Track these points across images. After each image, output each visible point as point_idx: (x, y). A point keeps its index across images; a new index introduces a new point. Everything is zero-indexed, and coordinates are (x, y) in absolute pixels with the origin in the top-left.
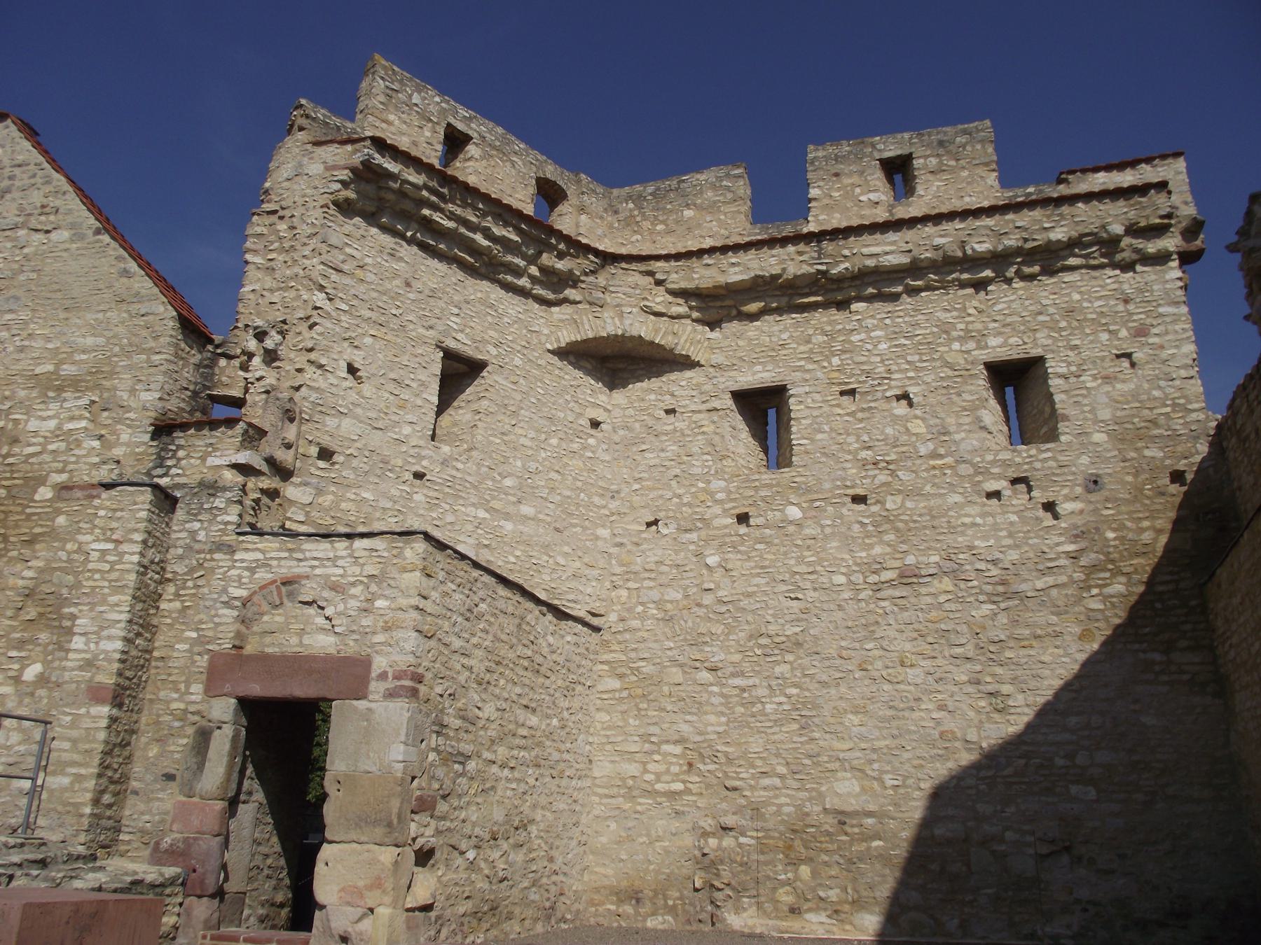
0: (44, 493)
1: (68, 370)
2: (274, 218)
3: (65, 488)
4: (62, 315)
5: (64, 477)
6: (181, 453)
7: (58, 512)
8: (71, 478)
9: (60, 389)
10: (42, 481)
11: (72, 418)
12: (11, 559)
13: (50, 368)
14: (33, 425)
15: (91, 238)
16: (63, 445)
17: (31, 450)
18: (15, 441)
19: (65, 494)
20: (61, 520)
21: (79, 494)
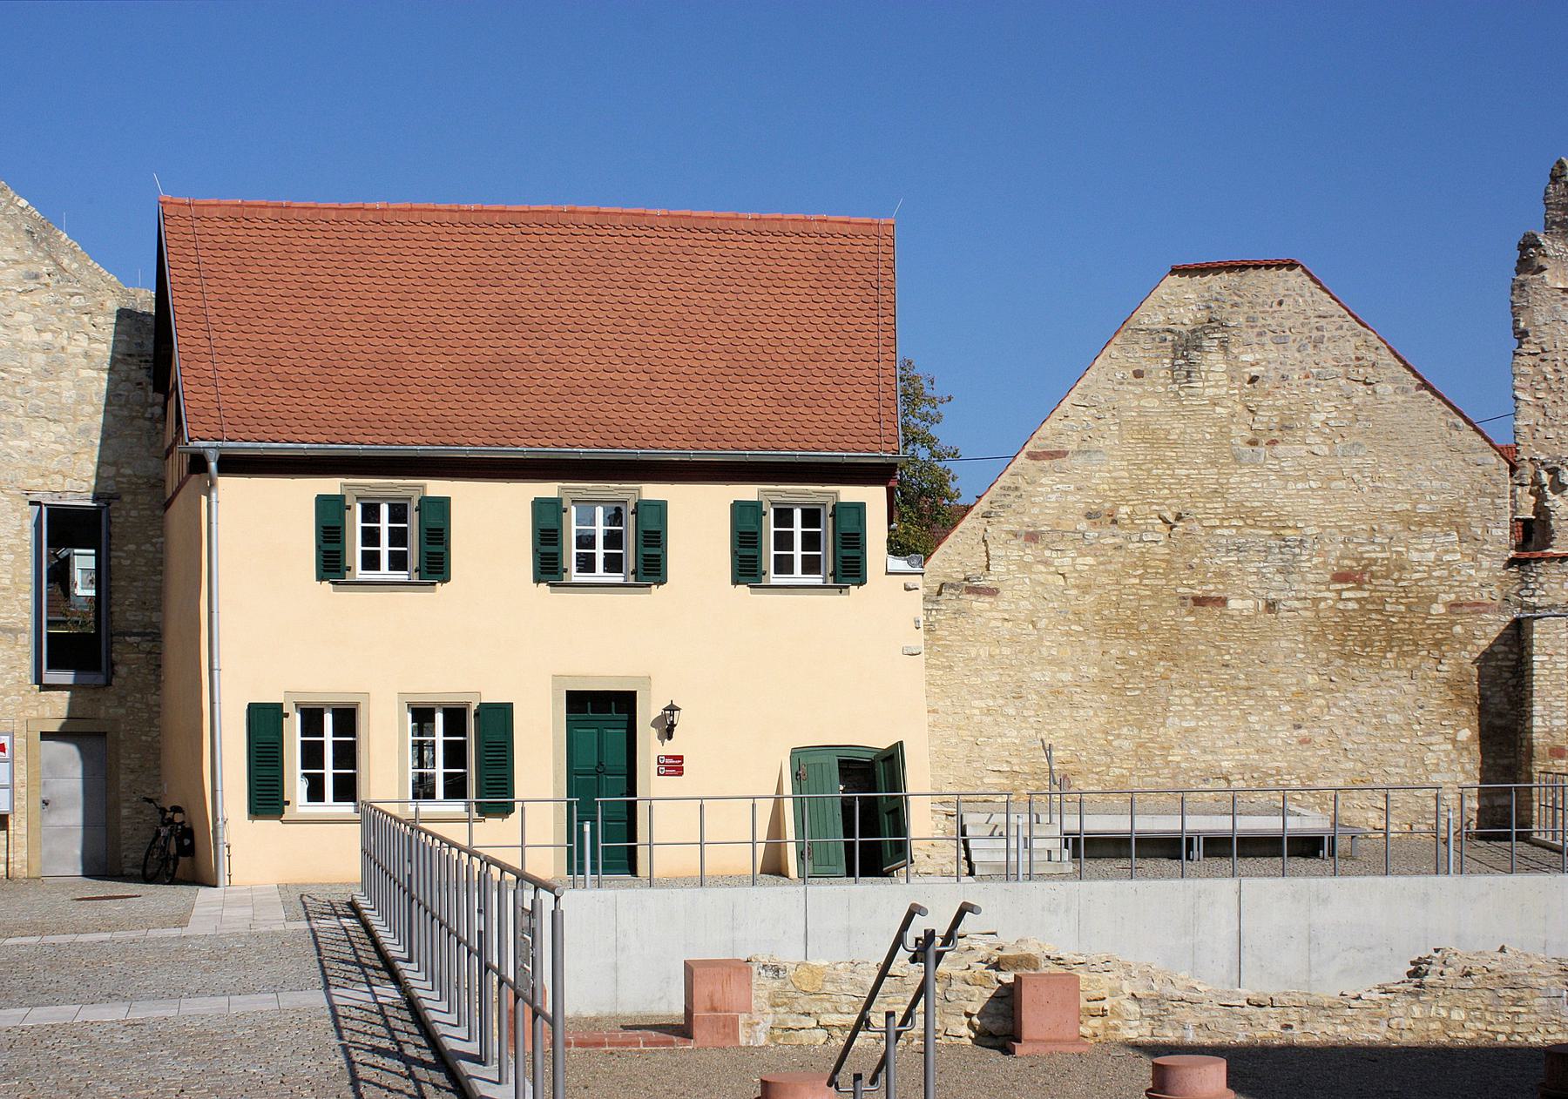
0: (1438, 609)
1: (1423, 508)
2: (1536, 359)
3: (1454, 606)
4: (1405, 461)
5: (1453, 596)
6: (1541, 579)
7: (1454, 623)
8: (1458, 598)
9: (1421, 524)
10: (1434, 599)
11: (1447, 552)
12: (1423, 657)
13: (1408, 506)
14: (1414, 556)
15: (1414, 393)
16: (1445, 573)
17: (1418, 576)
18: (1402, 568)
19: (1458, 610)
20: (1458, 629)
21: (1467, 610)
